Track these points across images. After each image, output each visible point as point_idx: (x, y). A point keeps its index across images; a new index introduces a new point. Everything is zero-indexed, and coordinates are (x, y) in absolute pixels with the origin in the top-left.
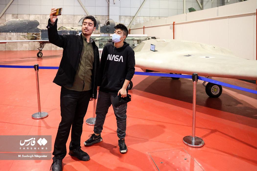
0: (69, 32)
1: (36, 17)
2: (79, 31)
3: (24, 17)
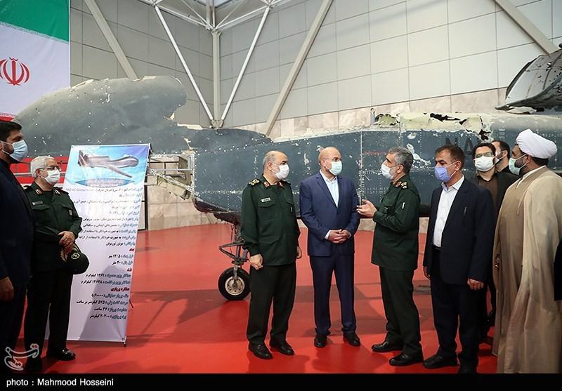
0: (411, 142)
1: (358, 117)
2: (496, 132)
3: (324, 120)
